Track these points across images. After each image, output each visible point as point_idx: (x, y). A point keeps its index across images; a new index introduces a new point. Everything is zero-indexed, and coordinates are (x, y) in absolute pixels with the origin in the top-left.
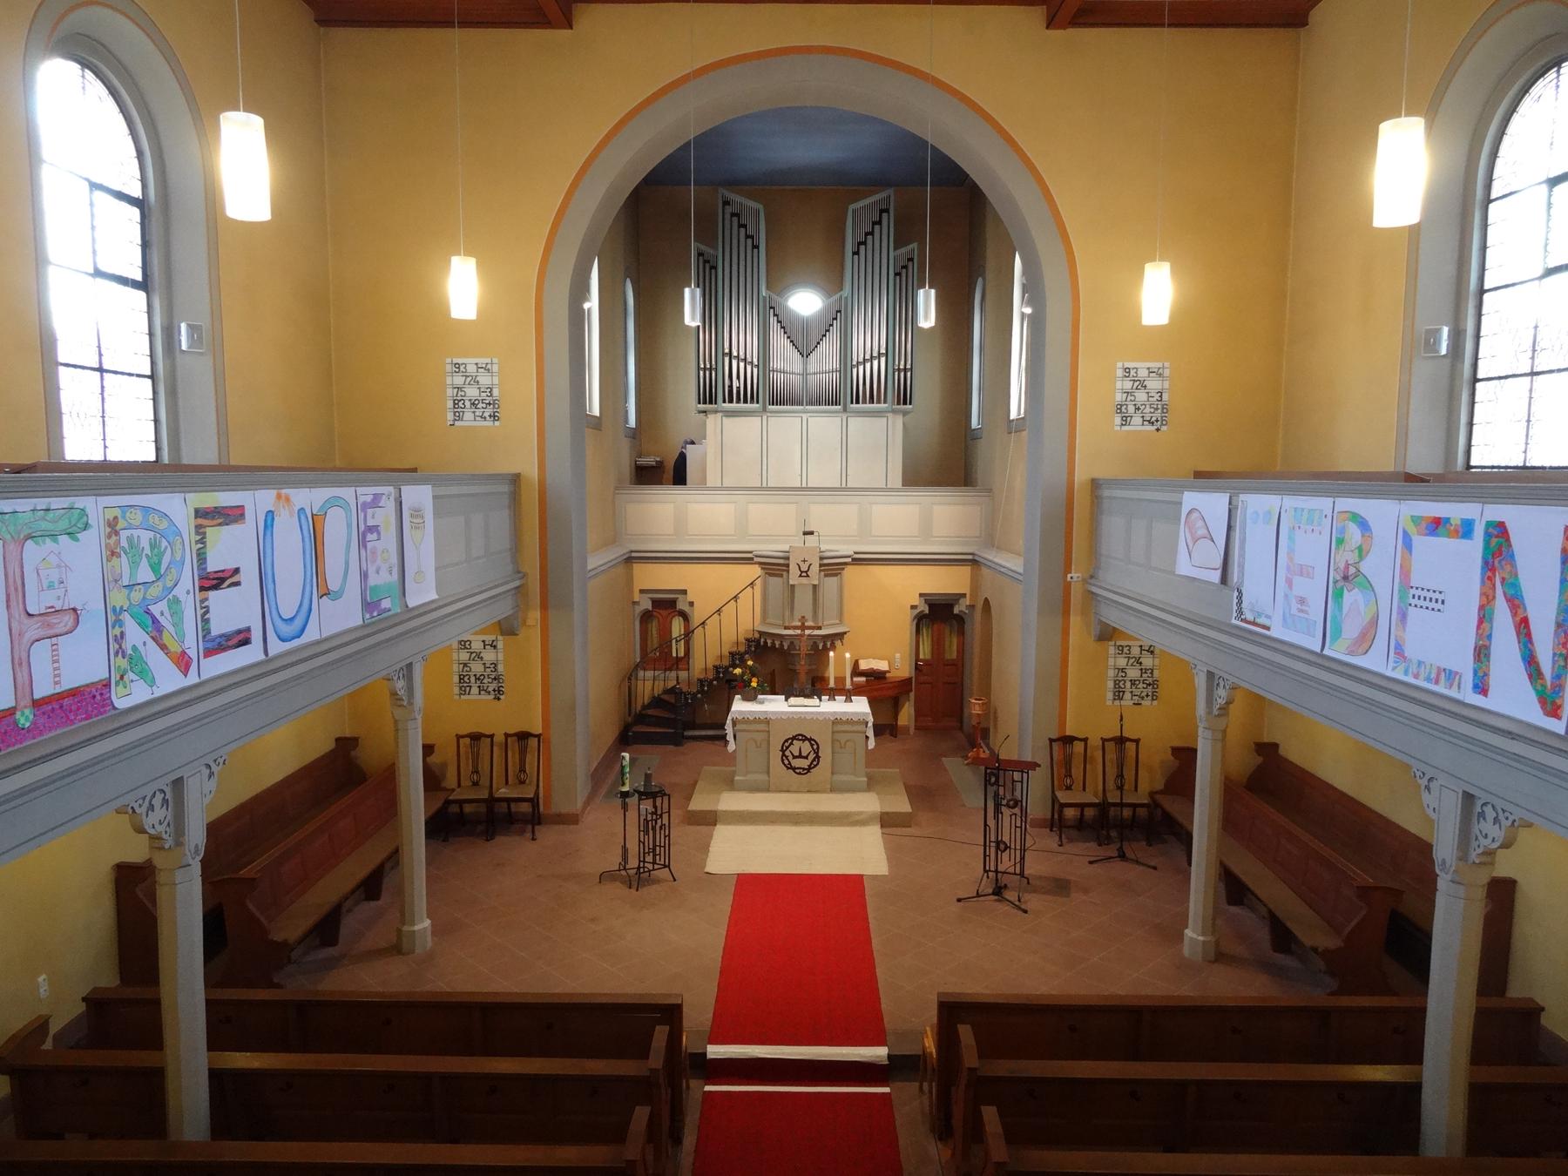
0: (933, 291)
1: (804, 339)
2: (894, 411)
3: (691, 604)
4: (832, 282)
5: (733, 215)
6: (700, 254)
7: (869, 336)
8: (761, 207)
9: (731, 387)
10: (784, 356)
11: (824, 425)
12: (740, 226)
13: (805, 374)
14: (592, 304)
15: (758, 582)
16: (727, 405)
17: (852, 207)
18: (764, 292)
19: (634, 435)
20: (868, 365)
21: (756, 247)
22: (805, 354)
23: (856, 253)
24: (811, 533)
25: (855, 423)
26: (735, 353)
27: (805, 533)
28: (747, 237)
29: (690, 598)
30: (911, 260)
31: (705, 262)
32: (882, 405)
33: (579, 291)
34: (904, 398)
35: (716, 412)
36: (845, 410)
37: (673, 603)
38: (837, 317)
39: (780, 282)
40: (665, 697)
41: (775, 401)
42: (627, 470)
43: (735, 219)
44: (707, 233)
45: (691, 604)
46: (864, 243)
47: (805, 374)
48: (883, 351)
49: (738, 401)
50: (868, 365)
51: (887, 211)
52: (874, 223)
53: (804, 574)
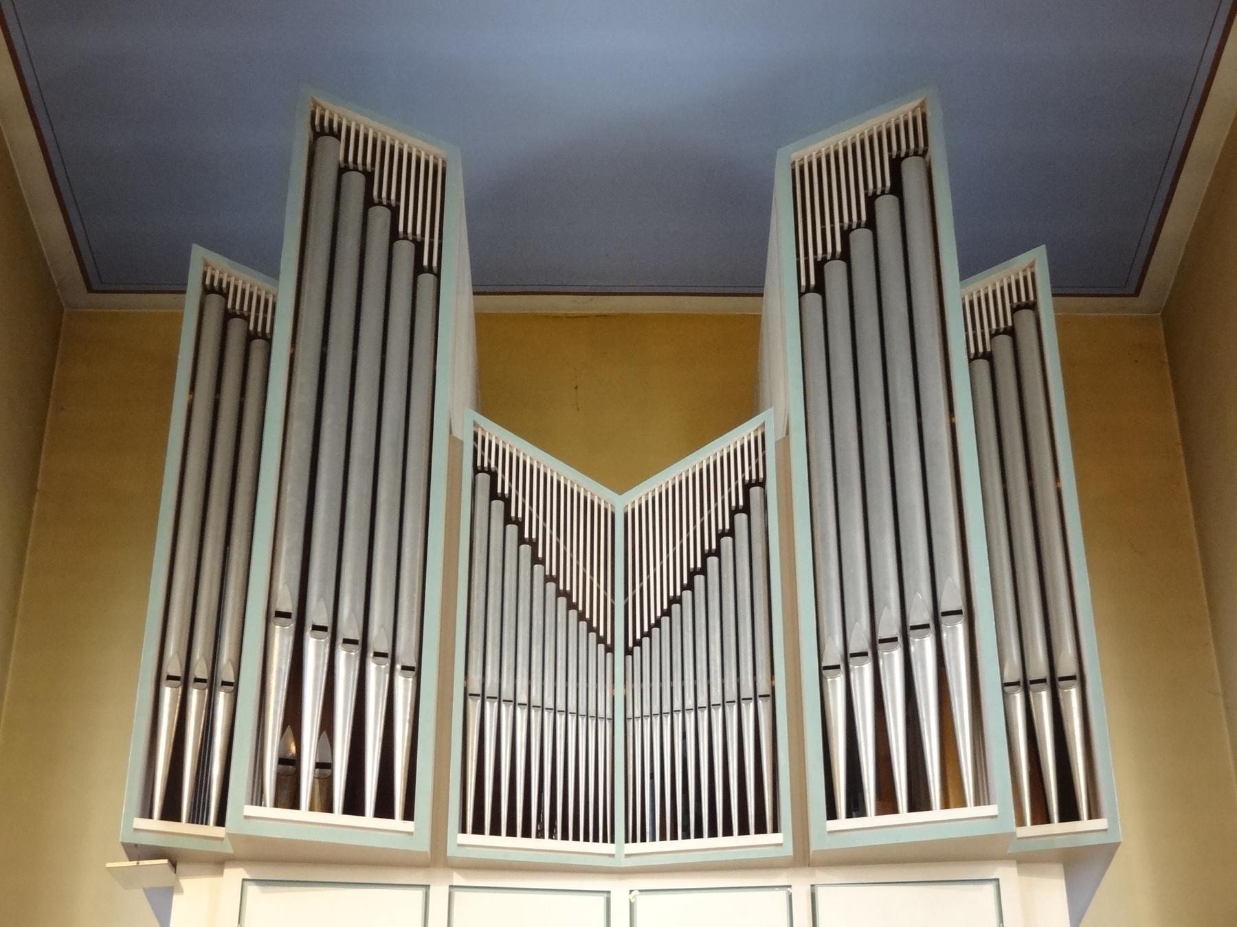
2: (1028, 860)
5: (342, 170)
6: (208, 290)
23: (820, 288)
26: (318, 612)
31: (228, 316)
35: (217, 863)
48: (951, 598)
50: (893, 660)
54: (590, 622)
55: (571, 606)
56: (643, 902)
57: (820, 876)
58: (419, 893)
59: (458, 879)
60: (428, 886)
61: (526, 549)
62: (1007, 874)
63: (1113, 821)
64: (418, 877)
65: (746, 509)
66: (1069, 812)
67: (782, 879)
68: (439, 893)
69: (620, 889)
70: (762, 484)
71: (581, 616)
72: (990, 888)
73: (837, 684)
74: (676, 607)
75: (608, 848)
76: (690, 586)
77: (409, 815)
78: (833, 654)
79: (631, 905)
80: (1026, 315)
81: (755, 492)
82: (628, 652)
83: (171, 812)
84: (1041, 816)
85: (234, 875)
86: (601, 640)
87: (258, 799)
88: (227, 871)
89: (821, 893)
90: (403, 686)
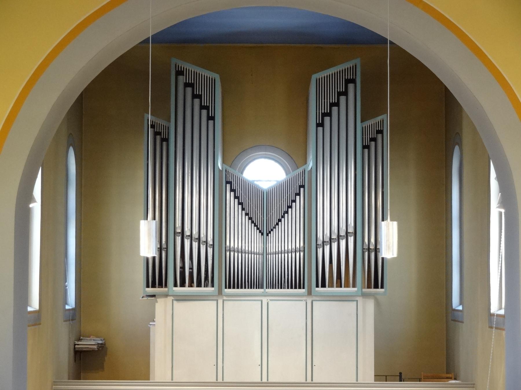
0: (395, 223)
1: (264, 213)
4: (294, 153)
5: (186, 85)
7: (335, 204)
8: (217, 77)
9: (183, 268)
10: (243, 239)
11: (286, 309)
12: (195, 96)
13: (265, 253)
14: (36, 207)
16: (179, 289)
17: (314, 77)
18: (219, 164)
19: (73, 316)
20: (335, 245)
21: (211, 118)
22: (266, 232)
25: (321, 308)
26: (187, 232)
28: (202, 107)
30: (380, 132)
31: (156, 134)
32: (351, 289)
33: (25, 196)
34: (376, 280)
35: (166, 295)
36: (310, 293)
38: (300, 188)
39: (237, 152)
41: (235, 281)
42: (65, 356)
43: (189, 90)
44: (161, 106)
46: (329, 114)
47: (265, 253)
48: (351, 230)
49: (191, 285)
50: (335, 245)
51: (353, 81)
52: (340, 94)
54: (257, 226)
55: (252, 222)
56: (270, 303)
57: (314, 298)
58: (215, 302)
59: (225, 298)
60: (217, 300)
61: (240, 206)
62: (360, 300)
63: (386, 290)
64: (215, 298)
65: (299, 194)
66: (376, 286)
67: (304, 298)
68: (220, 302)
69: (265, 300)
70: (303, 186)
71: (255, 224)
72: (355, 302)
73: (320, 251)
74: (280, 223)
75: (262, 290)
76: (283, 217)
77: (213, 286)
78: (320, 242)
79: (268, 303)
80: (380, 136)
81: (302, 189)
82: (267, 235)
83: (154, 286)
84: (369, 287)
85: (170, 299)
86: (260, 232)
87: (175, 285)
88: (168, 297)
89: (314, 302)
90: (210, 251)
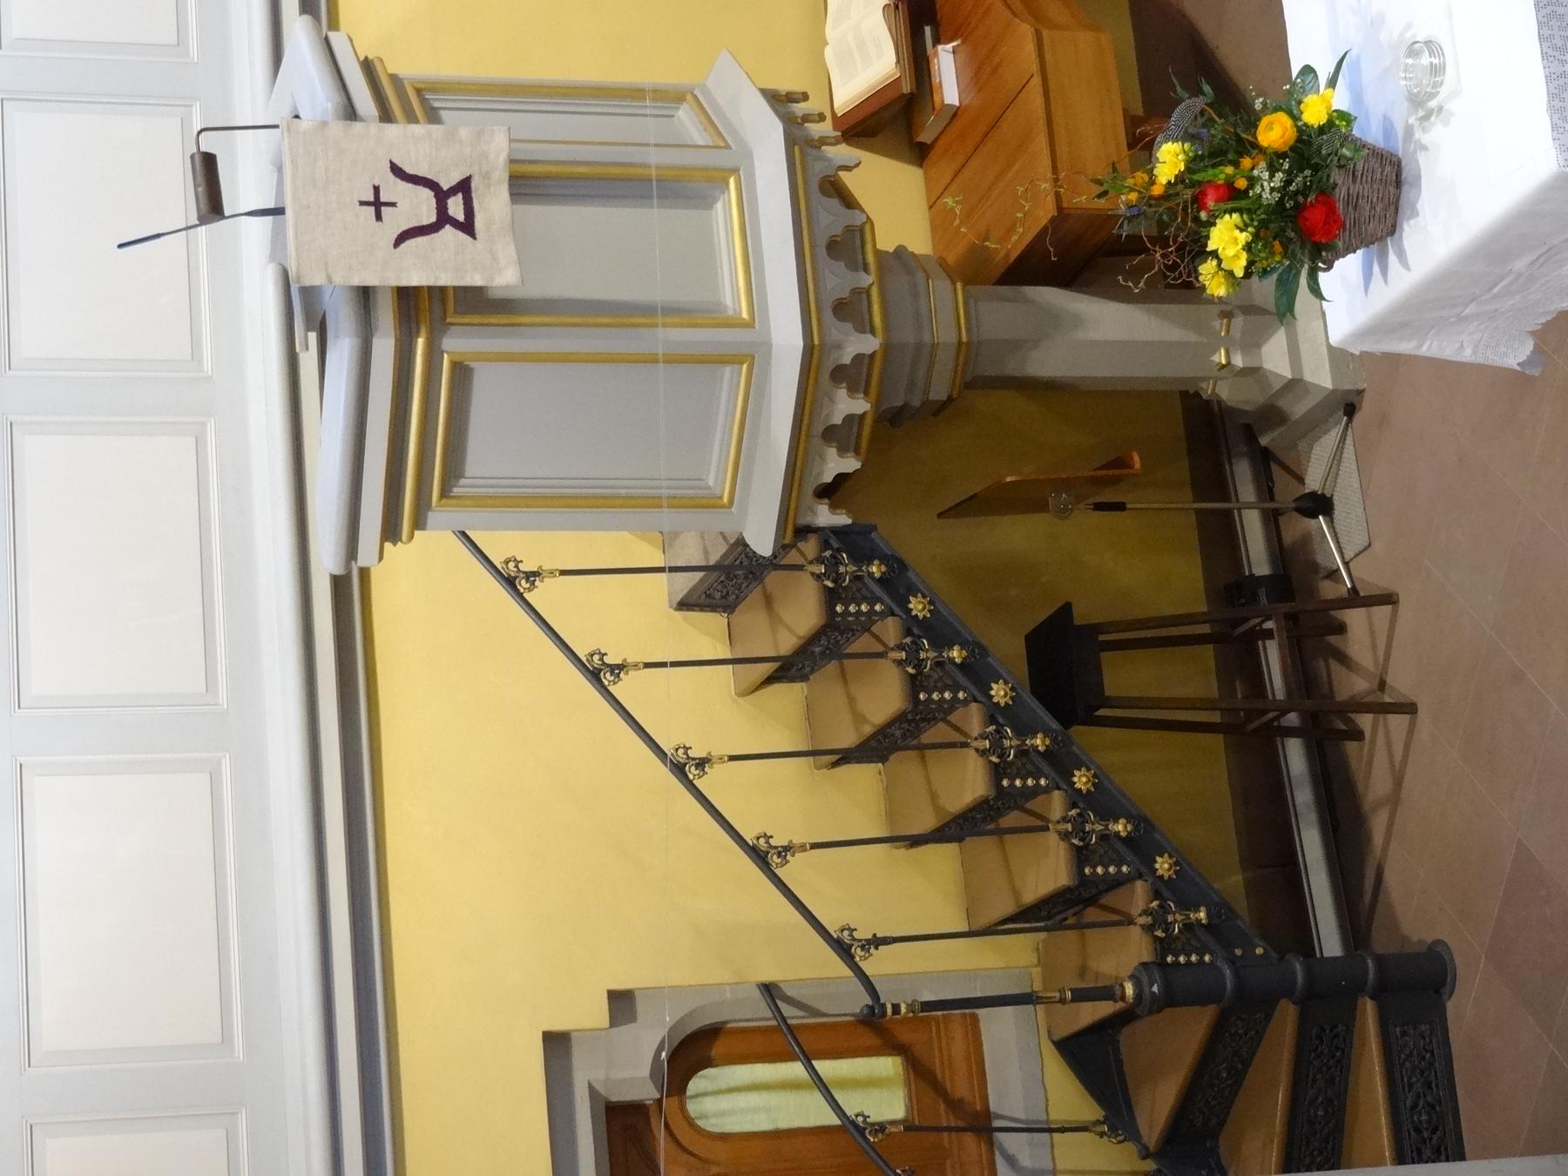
3: (622, 1003)
15: (501, 544)
24: (208, 166)
27: (212, 206)
29: (584, 1012)
37: (625, 1125)
40: (1157, 1105)
45: (622, 1003)
53: (453, 206)
